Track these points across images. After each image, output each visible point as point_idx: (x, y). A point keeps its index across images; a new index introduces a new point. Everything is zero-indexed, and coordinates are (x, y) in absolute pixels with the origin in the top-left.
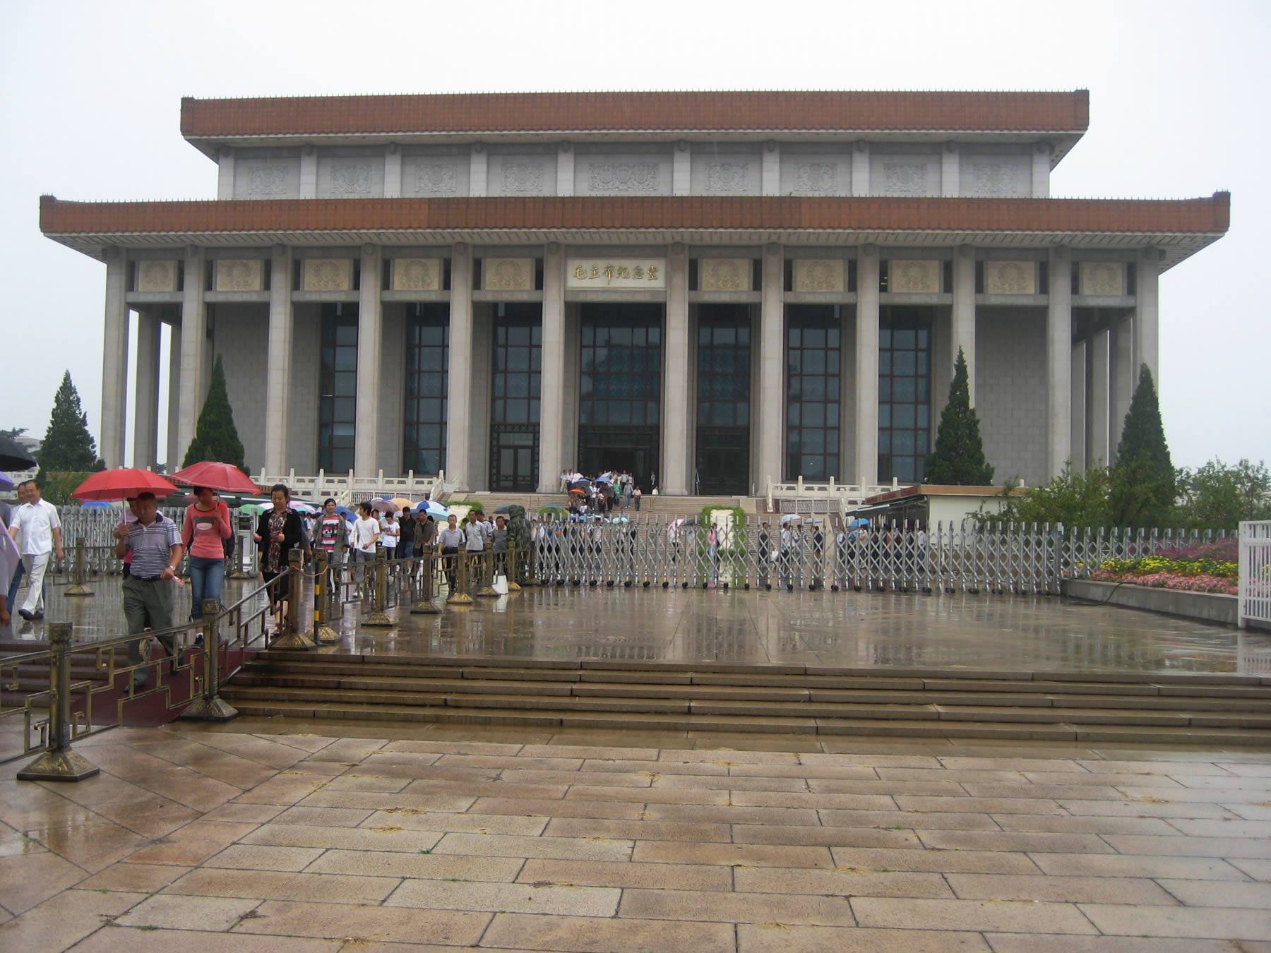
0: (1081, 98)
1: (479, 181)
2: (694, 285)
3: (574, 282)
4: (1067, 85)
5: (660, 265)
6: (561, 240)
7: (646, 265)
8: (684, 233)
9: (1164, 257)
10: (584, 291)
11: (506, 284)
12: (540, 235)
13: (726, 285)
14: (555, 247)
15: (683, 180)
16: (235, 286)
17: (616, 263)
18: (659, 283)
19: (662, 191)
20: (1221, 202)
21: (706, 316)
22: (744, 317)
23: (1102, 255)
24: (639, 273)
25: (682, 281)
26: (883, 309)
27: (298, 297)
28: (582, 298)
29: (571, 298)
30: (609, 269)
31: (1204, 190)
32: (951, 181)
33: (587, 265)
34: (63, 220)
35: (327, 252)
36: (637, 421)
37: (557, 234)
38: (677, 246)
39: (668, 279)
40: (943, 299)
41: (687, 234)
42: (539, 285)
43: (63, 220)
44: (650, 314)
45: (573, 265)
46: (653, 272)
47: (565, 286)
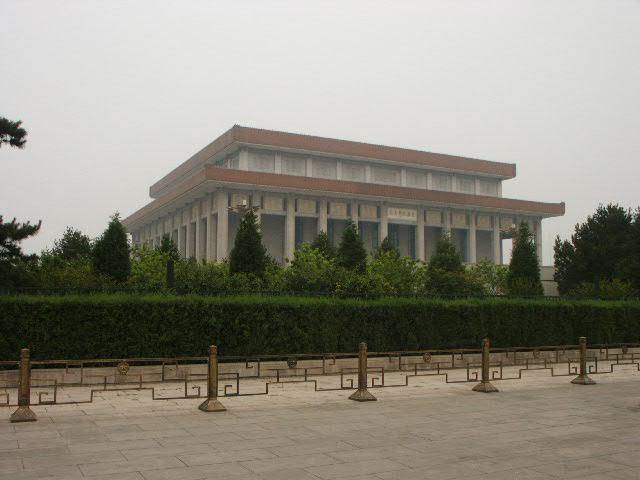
0: (513, 166)
3: (390, 216)
4: (511, 163)
5: (415, 212)
6: (390, 201)
7: (411, 211)
9: (541, 218)
10: (393, 220)
12: (382, 198)
14: (385, 203)
17: (403, 210)
18: (414, 218)
19: (396, 184)
24: (409, 215)
25: (422, 217)
26: (477, 231)
27: (297, 214)
32: (478, 190)
35: (307, 198)
37: (389, 199)
38: (421, 206)
39: (418, 217)
40: (376, 220)
41: (426, 203)
42: (379, 216)
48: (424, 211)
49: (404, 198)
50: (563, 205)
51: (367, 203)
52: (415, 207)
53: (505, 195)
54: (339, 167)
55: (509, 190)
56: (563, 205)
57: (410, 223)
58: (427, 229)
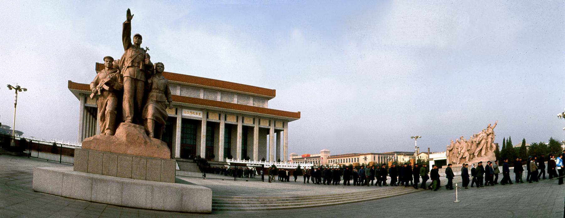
0: (274, 91)
2: (207, 117)
4: (273, 89)
5: (201, 113)
7: (199, 112)
8: (207, 107)
13: (214, 118)
15: (202, 95)
17: (193, 111)
21: (209, 124)
22: (217, 125)
23: (280, 120)
25: (205, 117)
32: (251, 103)
33: (186, 111)
36: (192, 143)
42: (176, 114)
44: (197, 123)
45: (184, 110)
48: (207, 113)
49: (194, 104)
50: (299, 113)
52: (201, 110)
53: (269, 108)
55: (271, 104)
56: (299, 113)
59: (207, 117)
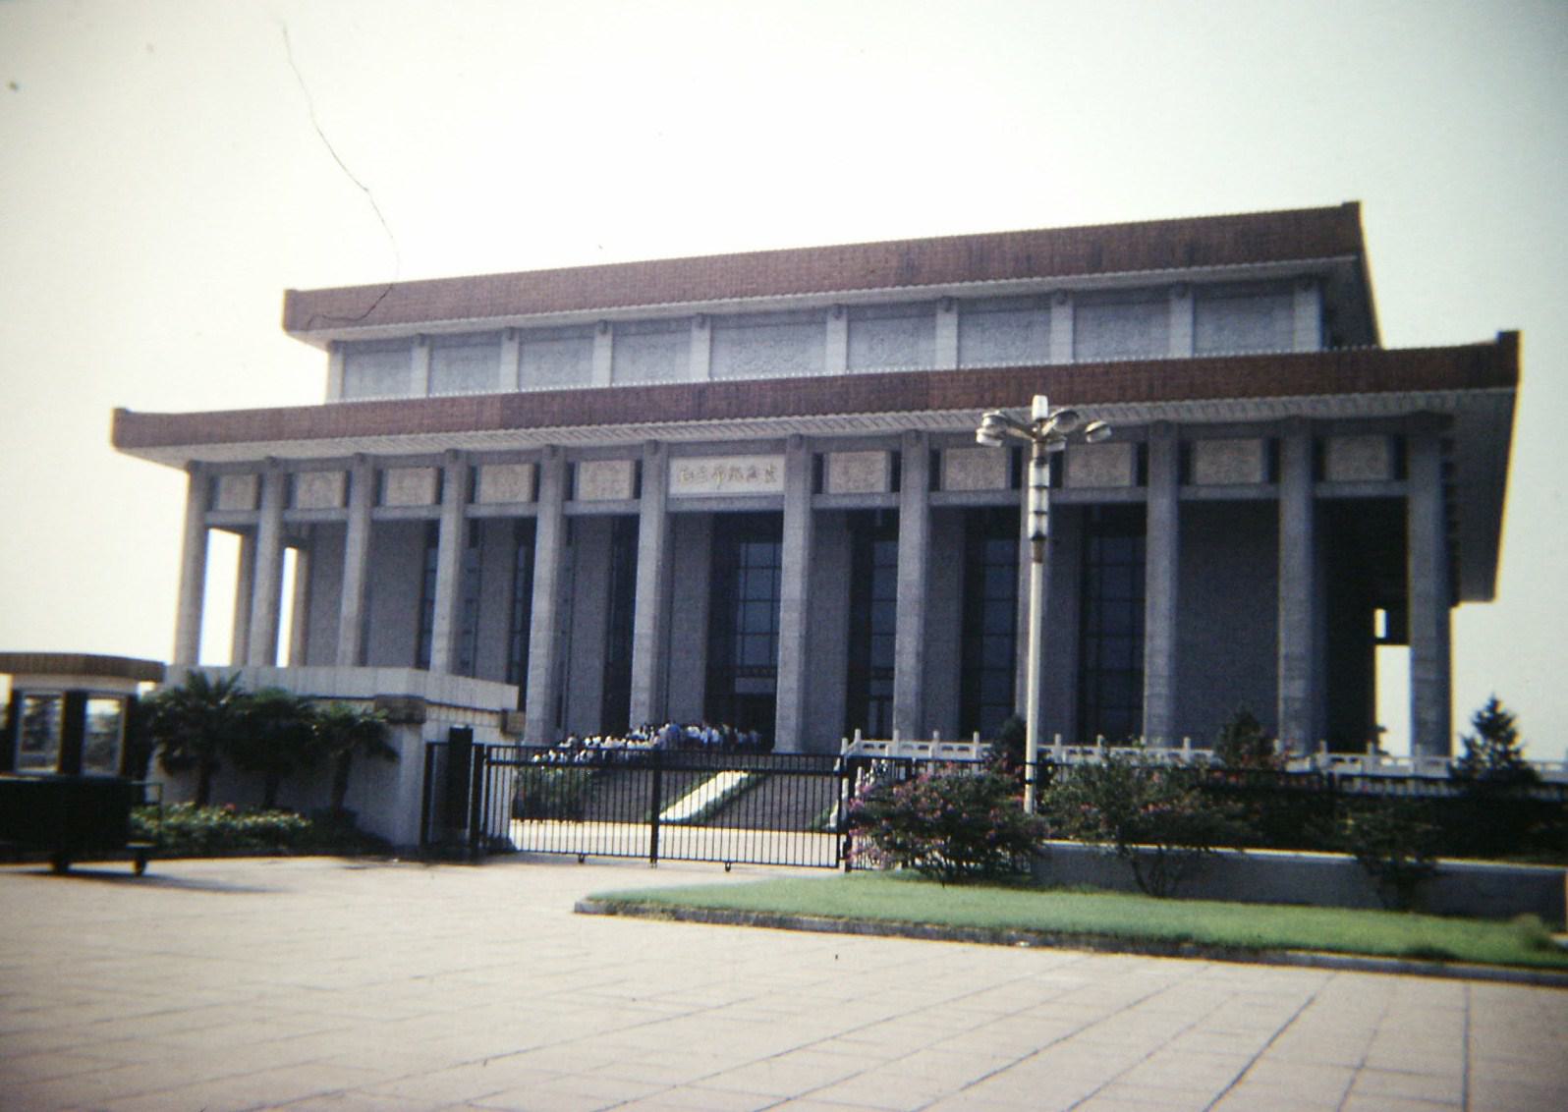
1: (598, 370)
2: (818, 485)
5: (779, 462)
7: (762, 463)
11: (603, 488)
14: (656, 445)
16: (318, 498)
17: (730, 462)
18: (777, 486)
20: (1508, 342)
24: (753, 475)
28: (686, 507)
29: (673, 508)
30: (720, 471)
31: (1480, 331)
33: (693, 464)
34: (136, 432)
42: (637, 493)
43: (136, 432)
45: (677, 466)
46: (769, 473)
47: (667, 494)
51: (596, 454)
52: (777, 446)
54: (602, 351)
57: (763, 505)
58: (823, 522)
59: (818, 485)
